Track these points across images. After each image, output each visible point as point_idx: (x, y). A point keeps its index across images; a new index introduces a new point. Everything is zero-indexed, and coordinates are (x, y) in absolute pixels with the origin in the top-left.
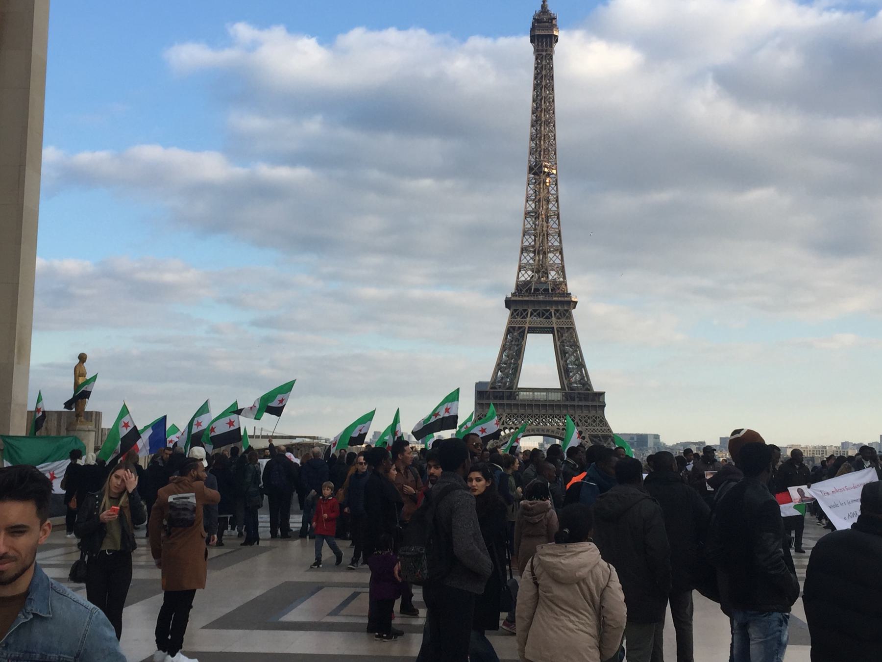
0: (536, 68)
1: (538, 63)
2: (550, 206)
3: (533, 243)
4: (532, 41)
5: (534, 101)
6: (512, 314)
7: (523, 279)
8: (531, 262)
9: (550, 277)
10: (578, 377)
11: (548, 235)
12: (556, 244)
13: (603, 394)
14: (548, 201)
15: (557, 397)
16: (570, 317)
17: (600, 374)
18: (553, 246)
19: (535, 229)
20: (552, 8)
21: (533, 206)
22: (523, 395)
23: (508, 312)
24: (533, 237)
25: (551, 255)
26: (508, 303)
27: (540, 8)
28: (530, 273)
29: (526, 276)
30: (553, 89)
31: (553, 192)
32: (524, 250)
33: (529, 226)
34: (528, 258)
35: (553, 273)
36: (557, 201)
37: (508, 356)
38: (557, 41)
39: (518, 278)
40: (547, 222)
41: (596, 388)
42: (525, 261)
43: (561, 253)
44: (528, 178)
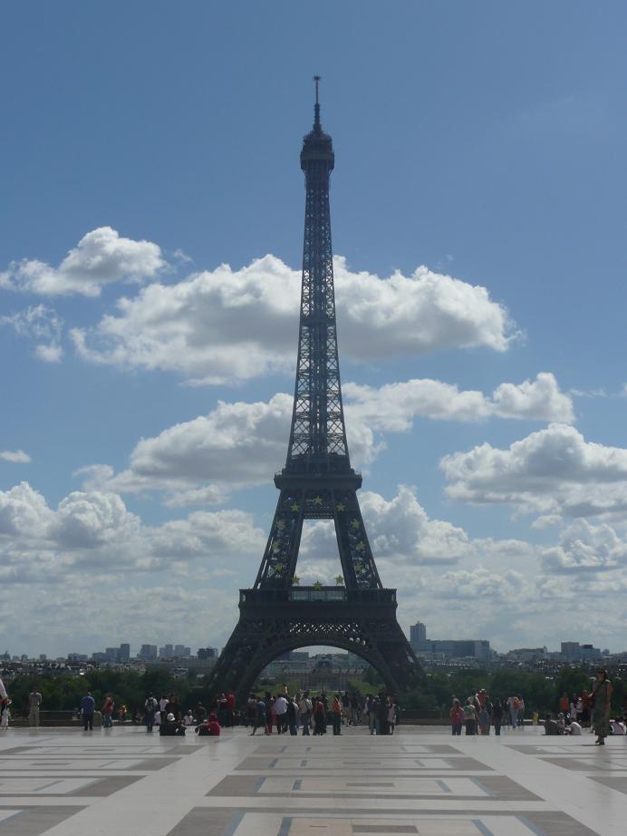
0: (308, 200)
1: (309, 193)
2: (328, 364)
3: (308, 410)
4: (302, 168)
5: (306, 239)
6: (282, 498)
7: (295, 453)
8: (306, 432)
9: (329, 450)
10: (363, 571)
11: (325, 400)
12: (337, 410)
13: (393, 592)
14: (327, 359)
15: (339, 597)
16: (354, 498)
17: (389, 572)
18: (334, 413)
19: (310, 392)
20: (327, 129)
21: (307, 364)
22: (297, 597)
23: (279, 491)
24: (308, 402)
25: (330, 423)
26: (278, 481)
27: (309, 129)
28: (305, 445)
29: (301, 449)
30: (329, 225)
31: (331, 347)
32: (296, 417)
33: (302, 388)
34: (303, 428)
35: (333, 444)
36: (337, 358)
37: (279, 547)
38: (333, 167)
39: (290, 450)
40: (326, 384)
41: (386, 584)
42: (298, 431)
43: (342, 421)
44: (301, 330)
